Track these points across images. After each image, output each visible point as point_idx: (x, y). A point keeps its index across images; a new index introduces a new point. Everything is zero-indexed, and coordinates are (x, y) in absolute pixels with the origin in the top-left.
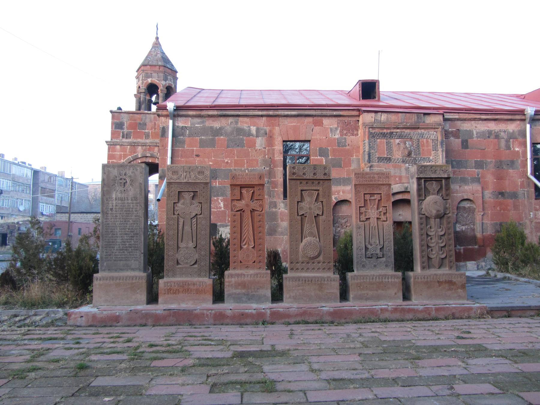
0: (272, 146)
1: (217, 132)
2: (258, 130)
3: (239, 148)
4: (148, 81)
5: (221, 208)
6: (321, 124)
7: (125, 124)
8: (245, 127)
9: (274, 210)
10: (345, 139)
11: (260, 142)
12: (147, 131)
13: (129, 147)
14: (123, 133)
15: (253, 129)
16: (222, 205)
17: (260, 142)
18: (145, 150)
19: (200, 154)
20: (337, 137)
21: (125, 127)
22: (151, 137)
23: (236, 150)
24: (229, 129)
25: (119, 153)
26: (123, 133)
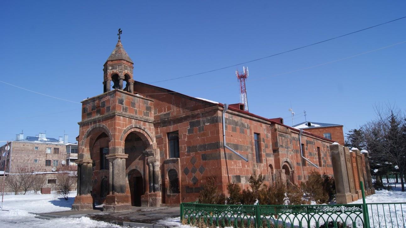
0: (251, 135)
1: (236, 124)
2: (247, 125)
3: (243, 134)
4: (125, 72)
5: (240, 167)
6: (261, 126)
7: (124, 101)
8: (244, 122)
9: (254, 168)
10: (268, 134)
11: (248, 131)
12: (136, 109)
13: (127, 118)
14: (123, 107)
15: (246, 124)
16: (241, 165)
17: (248, 131)
18: (136, 123)
19: (233, 135)
20: (266, 133)
21: (124, 103)
22: (138, 114)
23: (242, 134)
24: (239, 123)
25: (122, 122)
26: (123, 107)
